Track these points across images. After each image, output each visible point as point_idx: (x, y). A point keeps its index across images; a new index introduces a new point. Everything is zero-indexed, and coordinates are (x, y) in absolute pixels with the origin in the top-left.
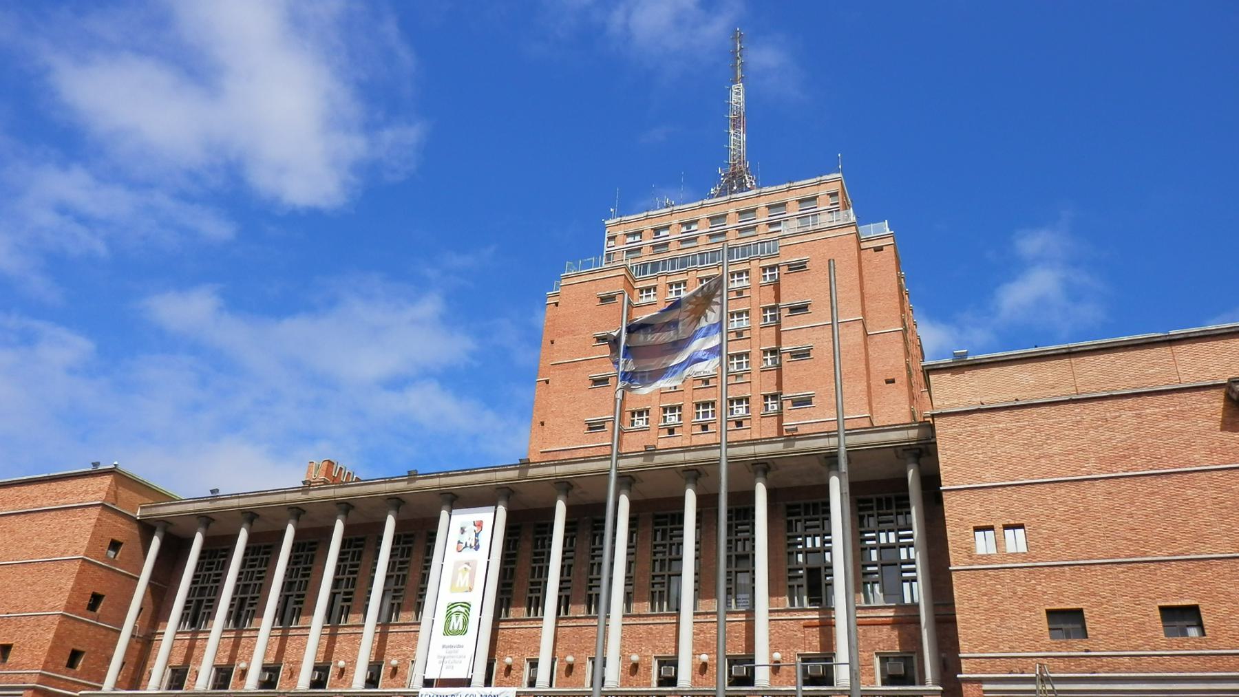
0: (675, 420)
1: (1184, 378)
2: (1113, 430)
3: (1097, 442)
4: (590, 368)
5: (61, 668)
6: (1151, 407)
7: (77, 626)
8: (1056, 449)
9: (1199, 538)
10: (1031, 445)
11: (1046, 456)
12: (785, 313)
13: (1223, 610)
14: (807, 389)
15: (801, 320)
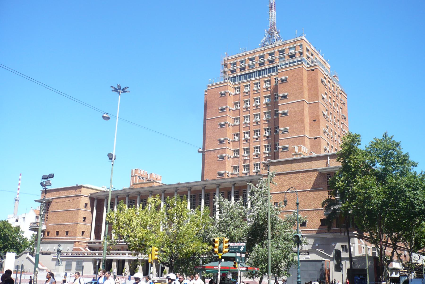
0: (247, 137)
1: (313, 167)
2: (297, 180)
3: (294, 183)
4: (218, 120)
5: (81, 236)
6: (305, 175)
7: (82, 225)
8: (286, 184)
9: (309, 205)
10: (281, 183)
11: (284, 186)
12: (280, 98)
13: (310, 221)
14: (287, 126)
15: (285, 102)
